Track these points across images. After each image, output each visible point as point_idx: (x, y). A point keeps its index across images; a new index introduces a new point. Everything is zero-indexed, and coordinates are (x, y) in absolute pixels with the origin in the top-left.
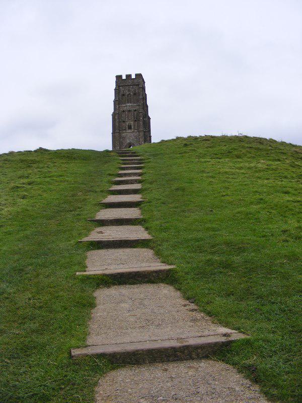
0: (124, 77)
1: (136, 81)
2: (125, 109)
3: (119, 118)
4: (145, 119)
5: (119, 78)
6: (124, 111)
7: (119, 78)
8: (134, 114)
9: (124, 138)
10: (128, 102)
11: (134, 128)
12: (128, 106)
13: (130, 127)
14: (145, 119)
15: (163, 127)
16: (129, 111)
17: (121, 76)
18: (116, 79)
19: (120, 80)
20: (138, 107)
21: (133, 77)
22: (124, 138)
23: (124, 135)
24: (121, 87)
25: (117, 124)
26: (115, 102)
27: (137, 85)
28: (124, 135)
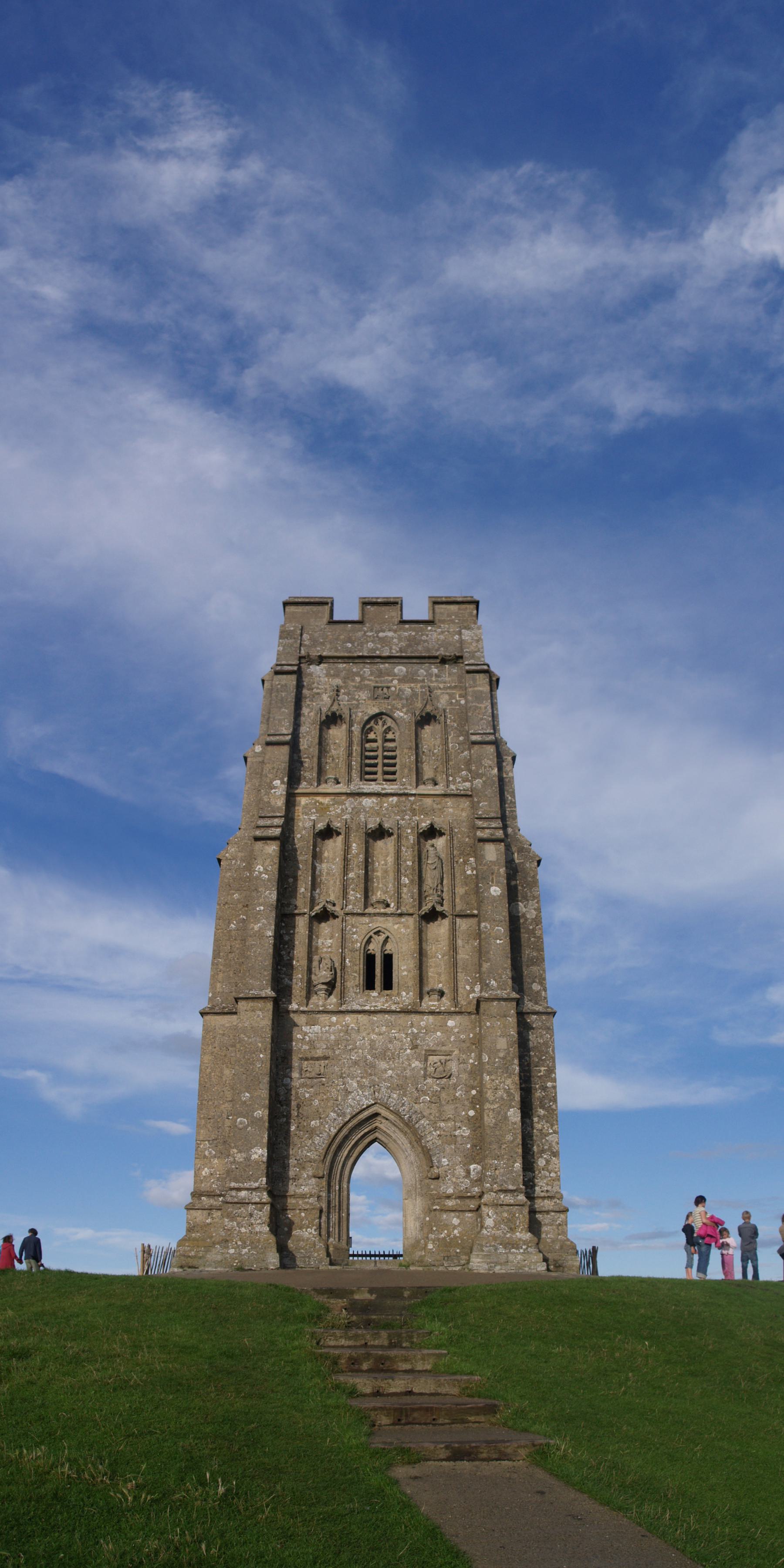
2: (339, 813)
13: (378, 972)
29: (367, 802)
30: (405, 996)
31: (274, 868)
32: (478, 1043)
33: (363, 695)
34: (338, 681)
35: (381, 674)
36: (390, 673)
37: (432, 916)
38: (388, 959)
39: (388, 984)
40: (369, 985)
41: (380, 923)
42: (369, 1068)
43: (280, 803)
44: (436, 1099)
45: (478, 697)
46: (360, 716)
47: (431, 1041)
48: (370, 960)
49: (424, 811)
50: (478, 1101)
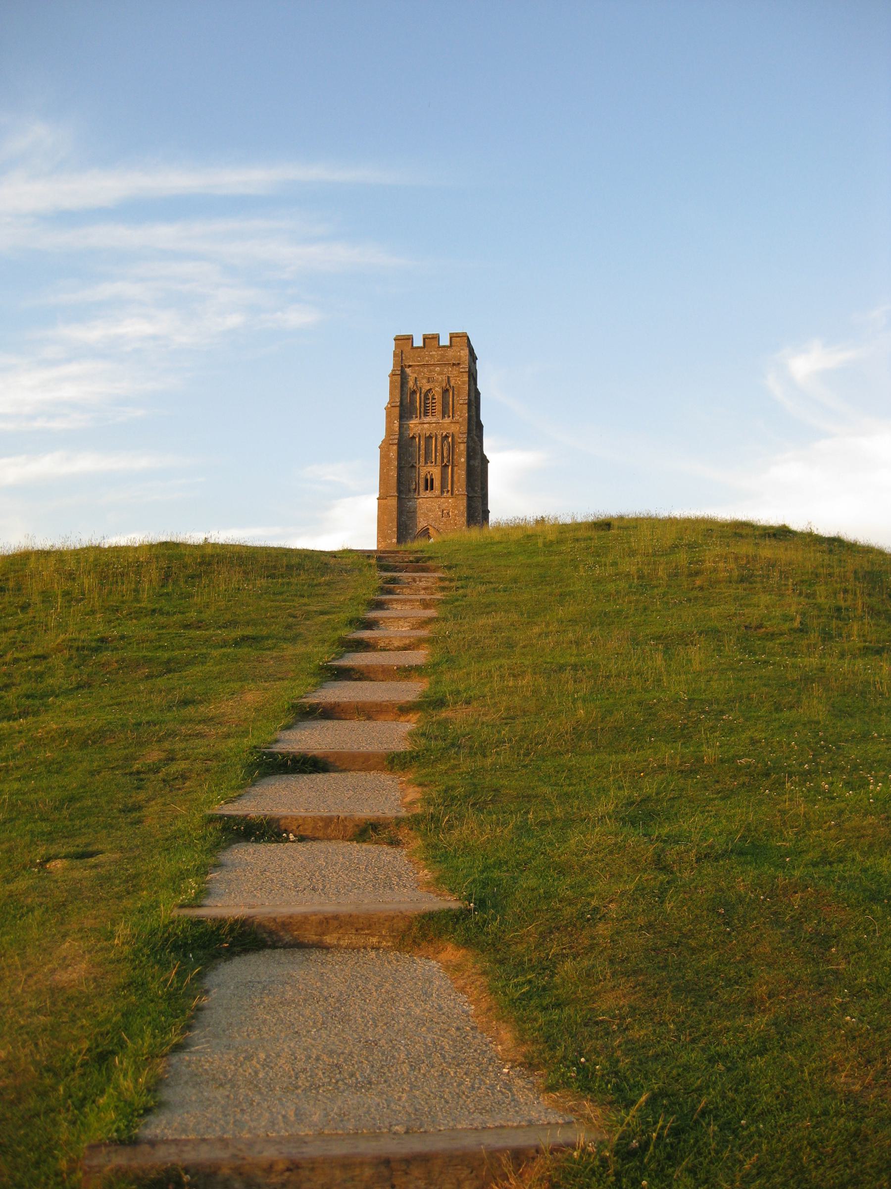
0: (418, 342)
1: (450, 353)
4: (472, 462)
5: (404, 341)
7: (404, 341)
13: (429, 485)
14: (472, 462)
15: (526, 485)
17: (410, 338)
18: (397, 346)
19: (407, 349)
21: (445, 341)
29: (426, 426)
31: (396, 455)
32: (455, 507)
33: (424, 381)
34: (415, 375)
35: (431, 371)
36: (435, 371)
38: (432, 480)
39: (432, 489)
41: (429, 469)
42: (426, 515)
43: (397, 429)
44: (445, 524)
45: (464, 383)
46: (423, 391)
47: (444, 506)
48: (427, 480)
49: (445, 429)
50: (456, 525)
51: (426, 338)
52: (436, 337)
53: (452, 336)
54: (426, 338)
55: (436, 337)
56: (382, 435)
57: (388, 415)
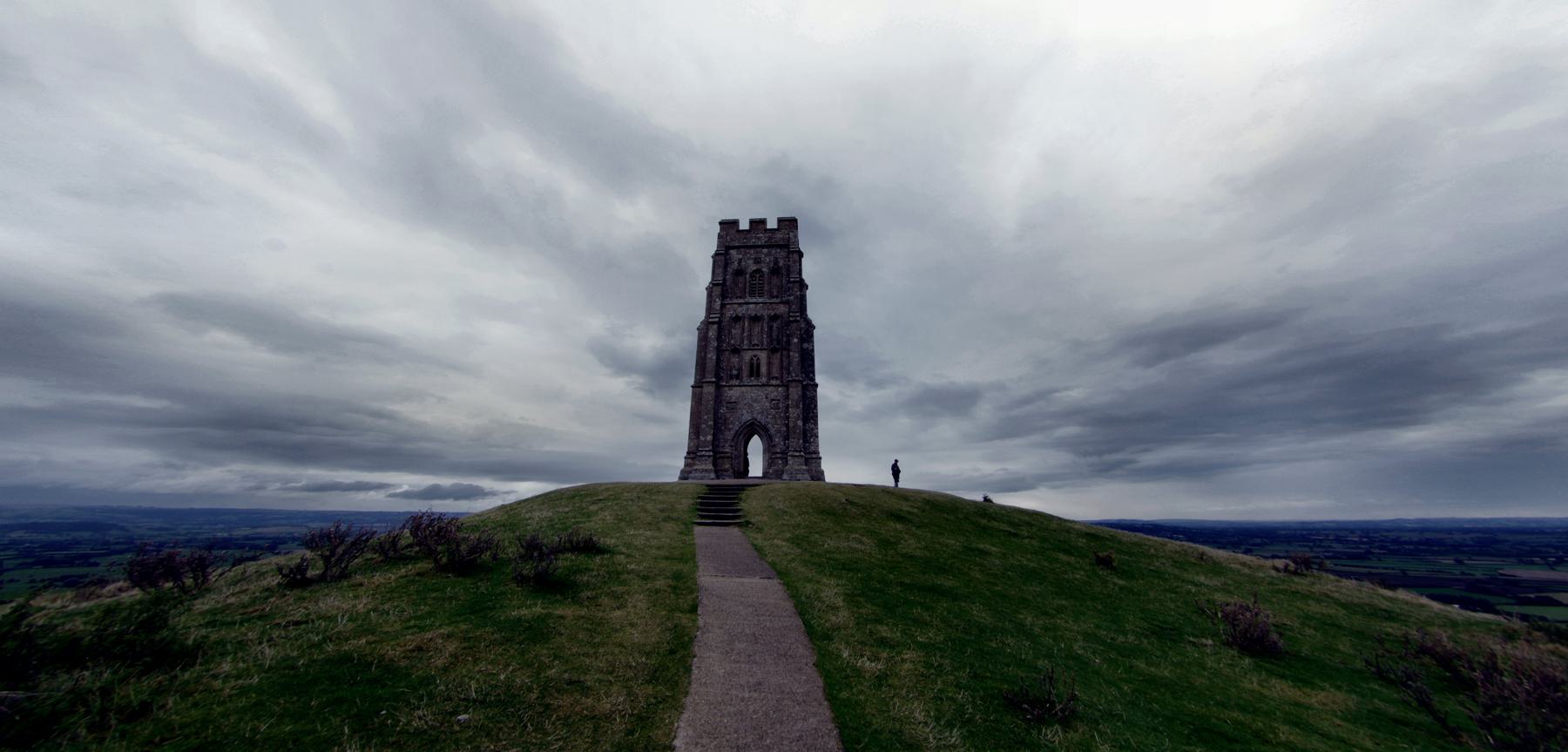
0: (744, 226)
1: (779, 235)
2: (741, 311)
3: (719, 338)
4: (805, 345)
5: (728, 226)
6: (737, 319)
7: (728, 226)
8: (770, 328)
9: (733, 406)
10: (752, 294)
11: (769, 373)
12: (754, 305)
16: (755, 319)
17: (735, 223)
20: (782, 309)
22: (733, 406)
23: (733, 393)
24: (733, 252)
25: (712, 356)
26: (710, 290)
27: (781, 247)
28: (733, 393)
30: (764, 380)
37: (773, 351)
38: (758, 365)
40: (751, 375)
42: (750, 406)
48: (752, 365)
51: (752, 222)
52: (763, 222)
53: (780, 221)
54: (752, 222)
55: (763, 222)
56: (701, 314)
57: (710, 296)
